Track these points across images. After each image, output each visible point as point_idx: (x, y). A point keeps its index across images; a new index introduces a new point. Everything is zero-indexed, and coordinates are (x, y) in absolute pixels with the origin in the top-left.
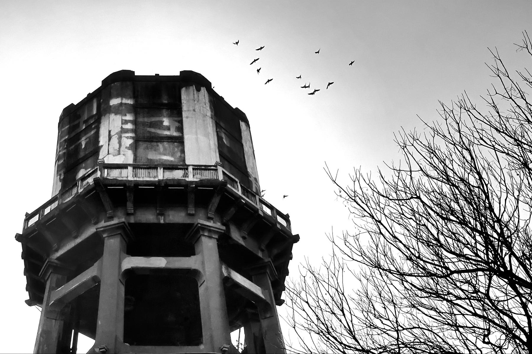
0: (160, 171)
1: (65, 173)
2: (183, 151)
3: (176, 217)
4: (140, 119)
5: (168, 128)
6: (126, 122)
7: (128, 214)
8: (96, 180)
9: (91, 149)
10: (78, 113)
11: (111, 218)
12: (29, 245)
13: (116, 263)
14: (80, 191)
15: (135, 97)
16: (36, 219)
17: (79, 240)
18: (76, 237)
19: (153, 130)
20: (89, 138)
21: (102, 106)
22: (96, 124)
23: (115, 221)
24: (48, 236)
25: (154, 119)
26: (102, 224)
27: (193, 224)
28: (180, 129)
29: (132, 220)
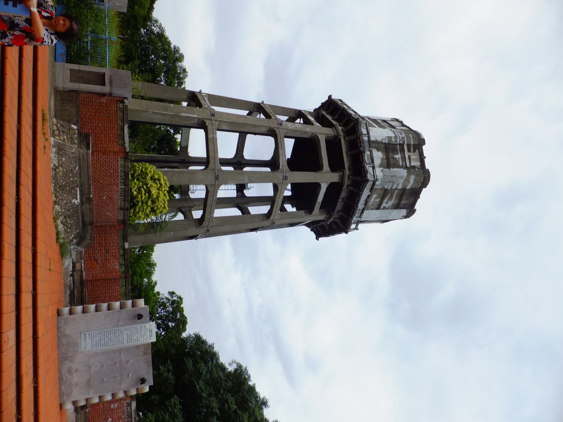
0: (363, 207)
1: (385, 143)
2: (372, 209)
3: (339, 206)
4: (396, 191)
5: (386, 203)
6: (398, 185)
7: (348, 186)
8: (367, 181)
9: (392, 161)
10: (417, 151)
11: (349, 178)
12: (352, 124)
13: (325, 178)
14: (367, 166)
15: (411, 189)
16: (364, 131)
17: (345, 155)
18: (347, 154)
21: (413, 170)
23: (346, 180)
24: (353, 137)
25: (394, 197)
26: (347, 172)
28: (384, 208)
29: (344, 188)
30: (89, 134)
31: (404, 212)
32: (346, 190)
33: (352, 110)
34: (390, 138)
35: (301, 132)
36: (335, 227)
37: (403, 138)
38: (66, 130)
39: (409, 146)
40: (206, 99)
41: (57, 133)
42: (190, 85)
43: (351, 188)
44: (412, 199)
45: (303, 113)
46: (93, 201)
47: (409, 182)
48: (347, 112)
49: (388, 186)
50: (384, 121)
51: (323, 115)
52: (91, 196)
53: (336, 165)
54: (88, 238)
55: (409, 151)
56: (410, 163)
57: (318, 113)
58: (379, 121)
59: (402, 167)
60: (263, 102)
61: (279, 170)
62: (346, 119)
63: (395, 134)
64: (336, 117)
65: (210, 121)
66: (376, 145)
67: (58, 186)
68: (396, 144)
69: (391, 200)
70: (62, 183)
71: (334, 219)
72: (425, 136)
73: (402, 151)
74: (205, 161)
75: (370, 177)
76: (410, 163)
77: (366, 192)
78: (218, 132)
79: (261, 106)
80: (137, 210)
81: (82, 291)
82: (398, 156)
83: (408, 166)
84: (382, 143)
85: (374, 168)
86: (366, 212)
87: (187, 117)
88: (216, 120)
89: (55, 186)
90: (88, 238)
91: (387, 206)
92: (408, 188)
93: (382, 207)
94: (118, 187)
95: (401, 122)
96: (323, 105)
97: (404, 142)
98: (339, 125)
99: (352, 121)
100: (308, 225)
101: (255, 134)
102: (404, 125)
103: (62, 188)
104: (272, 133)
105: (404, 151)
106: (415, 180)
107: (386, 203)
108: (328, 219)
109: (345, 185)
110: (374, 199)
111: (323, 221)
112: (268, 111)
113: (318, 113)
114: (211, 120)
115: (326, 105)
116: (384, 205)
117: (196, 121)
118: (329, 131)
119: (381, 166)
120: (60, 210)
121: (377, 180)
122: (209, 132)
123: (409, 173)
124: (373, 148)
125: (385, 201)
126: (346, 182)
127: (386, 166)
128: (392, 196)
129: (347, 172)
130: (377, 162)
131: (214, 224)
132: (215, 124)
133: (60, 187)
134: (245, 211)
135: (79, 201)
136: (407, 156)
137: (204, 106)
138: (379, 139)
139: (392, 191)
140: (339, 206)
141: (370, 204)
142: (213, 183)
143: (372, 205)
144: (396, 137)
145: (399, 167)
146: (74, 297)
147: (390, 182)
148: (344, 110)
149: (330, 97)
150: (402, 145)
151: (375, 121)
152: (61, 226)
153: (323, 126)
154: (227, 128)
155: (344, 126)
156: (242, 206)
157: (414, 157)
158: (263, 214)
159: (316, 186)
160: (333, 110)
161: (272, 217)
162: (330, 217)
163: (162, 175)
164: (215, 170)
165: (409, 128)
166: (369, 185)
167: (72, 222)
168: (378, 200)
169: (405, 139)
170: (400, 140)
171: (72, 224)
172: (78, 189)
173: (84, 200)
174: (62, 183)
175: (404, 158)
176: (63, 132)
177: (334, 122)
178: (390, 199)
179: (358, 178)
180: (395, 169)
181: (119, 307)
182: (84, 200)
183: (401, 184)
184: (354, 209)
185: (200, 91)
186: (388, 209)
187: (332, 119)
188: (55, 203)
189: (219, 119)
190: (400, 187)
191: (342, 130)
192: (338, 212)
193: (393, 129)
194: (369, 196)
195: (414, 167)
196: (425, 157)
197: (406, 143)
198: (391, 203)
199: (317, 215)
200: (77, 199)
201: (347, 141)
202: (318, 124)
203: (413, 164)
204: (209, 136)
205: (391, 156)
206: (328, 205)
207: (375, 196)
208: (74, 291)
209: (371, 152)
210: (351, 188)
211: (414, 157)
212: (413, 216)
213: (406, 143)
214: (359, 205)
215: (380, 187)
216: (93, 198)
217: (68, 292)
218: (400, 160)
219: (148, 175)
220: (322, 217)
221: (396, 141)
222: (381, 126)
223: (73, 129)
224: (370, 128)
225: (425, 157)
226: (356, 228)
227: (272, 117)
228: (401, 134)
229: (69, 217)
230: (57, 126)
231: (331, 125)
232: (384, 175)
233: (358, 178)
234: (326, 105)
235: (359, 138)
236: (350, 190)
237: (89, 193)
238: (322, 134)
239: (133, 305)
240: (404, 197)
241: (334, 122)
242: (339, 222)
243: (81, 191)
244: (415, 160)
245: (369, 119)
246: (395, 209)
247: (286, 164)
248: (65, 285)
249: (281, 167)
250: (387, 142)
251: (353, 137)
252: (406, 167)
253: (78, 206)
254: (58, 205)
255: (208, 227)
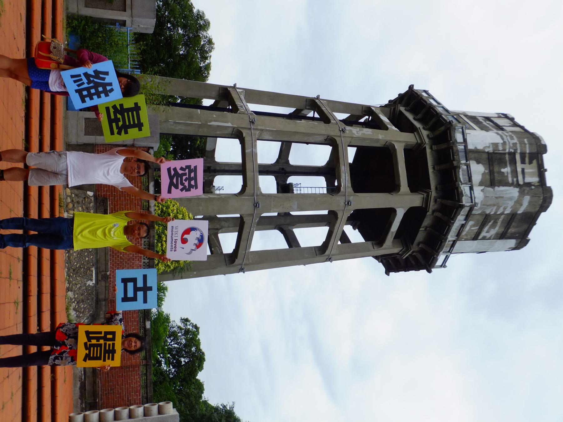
1: (488, 153)
3: (421, 236)
4: (503, 217)
6: (505, 209)
7: (434, 211)
8: (462, 207)
9: (497, 177)
10: (535, 162)
11: (435, 201)
12: (443, 128)
13: (402, 201)
15: (525, 214)
16: (459, 137)
18: (434, 168)
19: (490, 224)
20: (507, 176)
21: (528, 189)
22: (515, 182)
24: (443, 146)
25: (499, 223)
26: (433, 194)
27: (412, 244)
28: (484, 238)
29: (428, 213)
30: (107, 199)
31: (512, 243)
32: (432, 217)
33: (443, 107)
34: (496, 145)
35: (371, 140)
36: (413, 262)
37: (515, 144)
38: (80, 200)
39: (523, 155)
40: (242, 97)
41: (71, 206)
42: (220, 74)
43: (438, 214)
44: (525, 227)
45: (373, 111)
46: (110, 278)
47: (521, 205)
48: (436, 112)
49: (490, 211)
50: (488, 119)
51: (401, 112)
52: (108, 273)
53: (418, 183)
54: (102, 316)
55: (523, 162)
56: (524, 178)
57: (394, 109)
58: (481, 119)
59: (512, 185)
60: (318, 97)
61: (340, 194)
62: (434, 120)
63: (503, 139)
64: (419, 116)
65: (248, 131)
66: (476, 155)
67: (71, 270)
68: (505, 154)
69: (494, 228)
70: (76, 265)
71: (413, 252)
72: (546, 139)
73: (513, 162)
74: (241, 168)
75: (465, 201)
76: (524, 178)
77: (460, 219)
78: (258, 141)
79: (316, 103)
80: (156, 262)
81: (95, 382)
82: (507, 170)
83: (521, 182)
84: (484, 152)
85: (471, 188)
86: (458, 244)
87: (218, 126)
88: (257, 129)
89: (69, 270)
90: (102, 316)
91: (488, 235)
92: (519, 212)
93: (480, 237)
94: (141, 261)
95: (512, 119)
96: (401, 96)
97: (516, 150)
98: (424, 128)
99: (443, 124)
100: (376, 258)
101: (307, 143)
102: (516, 125)
103: (76, 271)
104: (330, 141)
105: (515, 163)
106: (530, 202)
107: (487, 232)
108: (404, 252)
109: (430, 211)
110: (471, 227)
111: (398, 254)
112: (325, 111)
113: (394, 109)
114: (250, 129)
115: (406, 98)
116: (483, 234)
117: (230, 131)
118: (409, 138)
119: (481, 184)
120: (72, 297)
121: (475, 204)
122: (246, 146)
123: (522, 193)
124: (471, 159)
125: (486, 229)
126: (432, 206)
127: (488, 183)
128: (495, 223)
129: (433, 194)
130: (477, 178)
131: (251, 262)
132: (255, 134)
133: (74, 270)
134: (291, 240)
135: (94, 282)
136: (519, 170)
137: (241, 110)
138: (480, 147)
139: (496, 217)
140: (421, 236)
141: (464, 233)
142: (250, 211)
143: (466, 235)
144: (504, 143)
145: (507, 184)
146: (85, 390)
147: (494, 205)
148: (431, 107)
149: (411, 87)
150: (512, 155)
151: (474, 119)
152: (73, 313)
153: (402, 130)
154: (271, 138)
155: (431, 129)
156: (285, 228)
157: (531, 170)
158: (315, 247)
159: (391, 212)
160: (413, 106)
161: (327, 252)
162: (407, 250)
163: (187, 213)
164: (253, 195)
165: (522, 128)
166: (464, 212)
167: (86, 305)
168: (476, 228)
169: (518, 146)
170: (510, 148)
171: (84, 308)
172: (93, 269)
173: (100, 278)
174: (76, 265)
175: (515, 173)
176: (78, 202)
177: (417, 125)
178: (493, 226)
179: (449, 202)
180: (502, 188)
181: (143, 414)
182: (100, 278)
183: (510, 207)
184: (442, 242)
185: (235, 85)
186: (489, 239)
187: (414, 119)
188: (68, 289)
189: (259, 128)
190: (508, 211)
191: (428, 136)
192: (419, 244)
193: (500, 132)
194: (463, 226)
195: (529, 184)
196: (546, 170)
197: (519, 151)
198: (493, 232)
199: (390, 247)
200: (92, 280)
201: (435, 151)
202: (394, 128)
203: (528, 179)
204: (246, 151)
205: (496, 169)
206: (406, 234)
207: (471, 223)
208: (85, 383)
209: (468, 166)
210: (438, 214)
211: (531, 170)
212: (525, 248)
213: (519, 151)
214: (449, 237)
215: (480, 212)
216: (110, 274)
217: (78, 385)
218: (510, 176)
219: (169, 215)
220: (396, 250)
221: (505, 150)
222: (483, 128)
223: (89, 197)
224: (467, 131)
225: (546, 170)
226: (443, 265)
227: (332, 121)
228: (512, 138)
229: (83, 301)
230: (71, 197)
231: (411, 129)
232: (486, 197)
233: (449, 202)
234: (406, 98)
235: (452, 148)
236: (436, 217)
237: (106, 271)
238: (400, 142)
239: (160, 411)
240: (513, 224)
241: (417, 125)
242: (419, 256)
243: (97, 269)
244: (531, 175)
245: (466, 116)
246: (499, 239)
247: (350, 185)
248: (75, 376)
249: (342, 189)
250: (491, 151)
251: (443, 146)
252: (518, 185)
253: (93, 287)
254: (71, 291)
255: (241, 265)
